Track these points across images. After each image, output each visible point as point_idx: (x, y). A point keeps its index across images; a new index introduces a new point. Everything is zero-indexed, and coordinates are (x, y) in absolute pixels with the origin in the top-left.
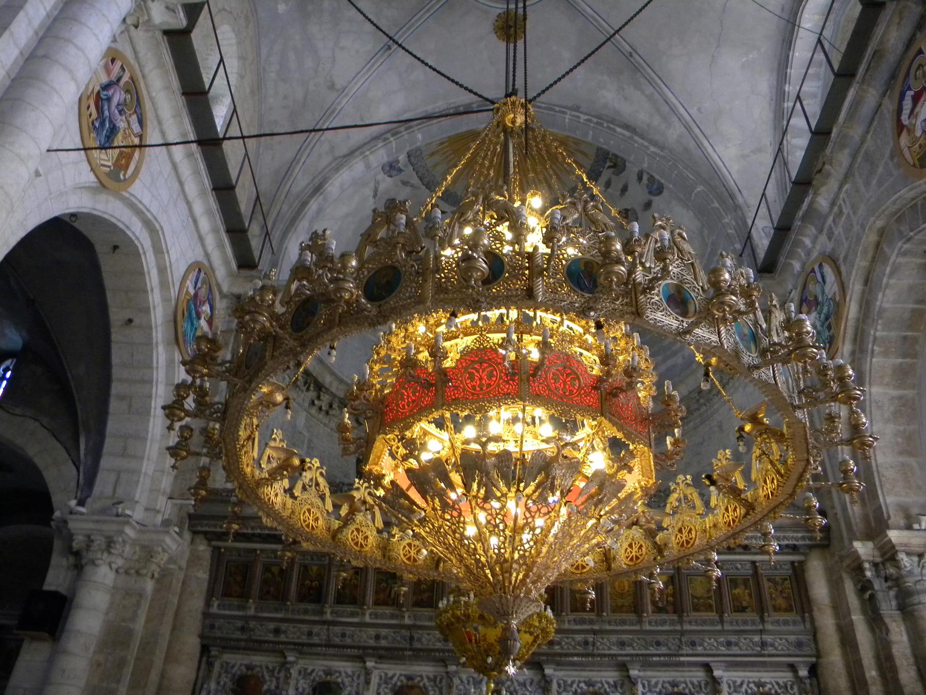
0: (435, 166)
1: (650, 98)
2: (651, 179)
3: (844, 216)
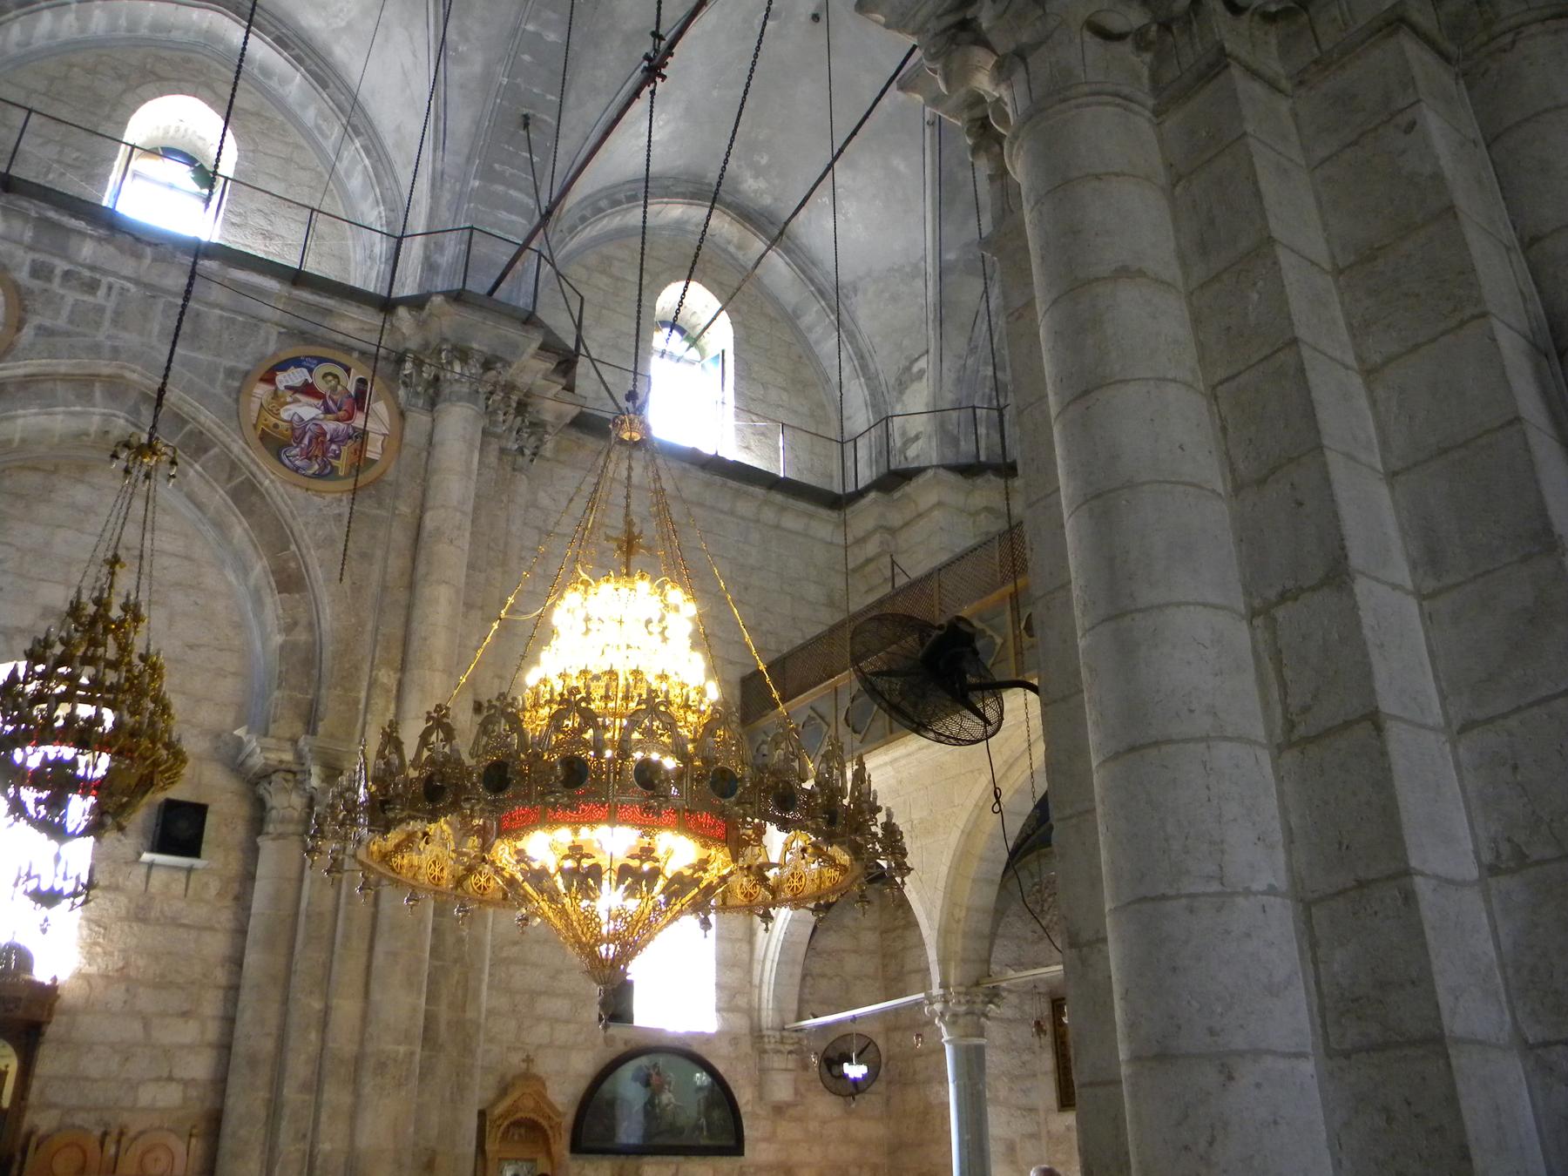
3: (86, 298)
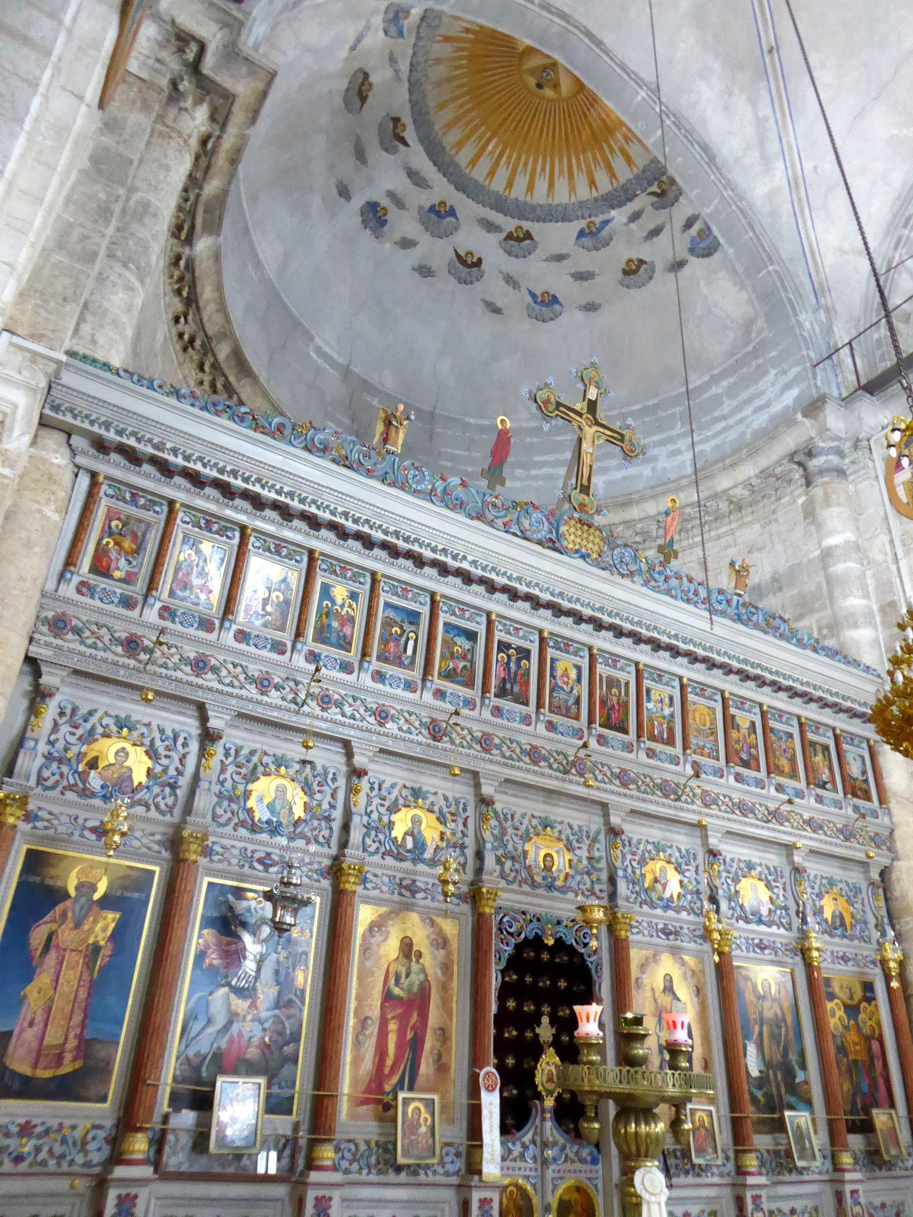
0: (438, 61)
1: (760, 123)
2: (706, 232)
